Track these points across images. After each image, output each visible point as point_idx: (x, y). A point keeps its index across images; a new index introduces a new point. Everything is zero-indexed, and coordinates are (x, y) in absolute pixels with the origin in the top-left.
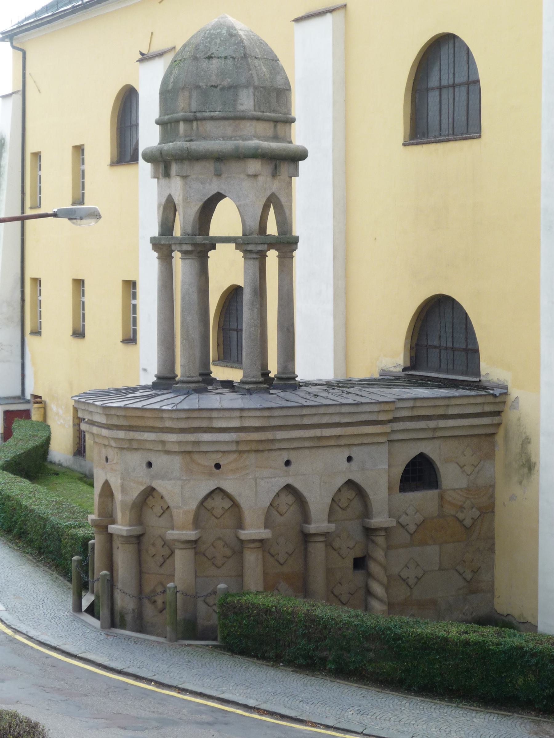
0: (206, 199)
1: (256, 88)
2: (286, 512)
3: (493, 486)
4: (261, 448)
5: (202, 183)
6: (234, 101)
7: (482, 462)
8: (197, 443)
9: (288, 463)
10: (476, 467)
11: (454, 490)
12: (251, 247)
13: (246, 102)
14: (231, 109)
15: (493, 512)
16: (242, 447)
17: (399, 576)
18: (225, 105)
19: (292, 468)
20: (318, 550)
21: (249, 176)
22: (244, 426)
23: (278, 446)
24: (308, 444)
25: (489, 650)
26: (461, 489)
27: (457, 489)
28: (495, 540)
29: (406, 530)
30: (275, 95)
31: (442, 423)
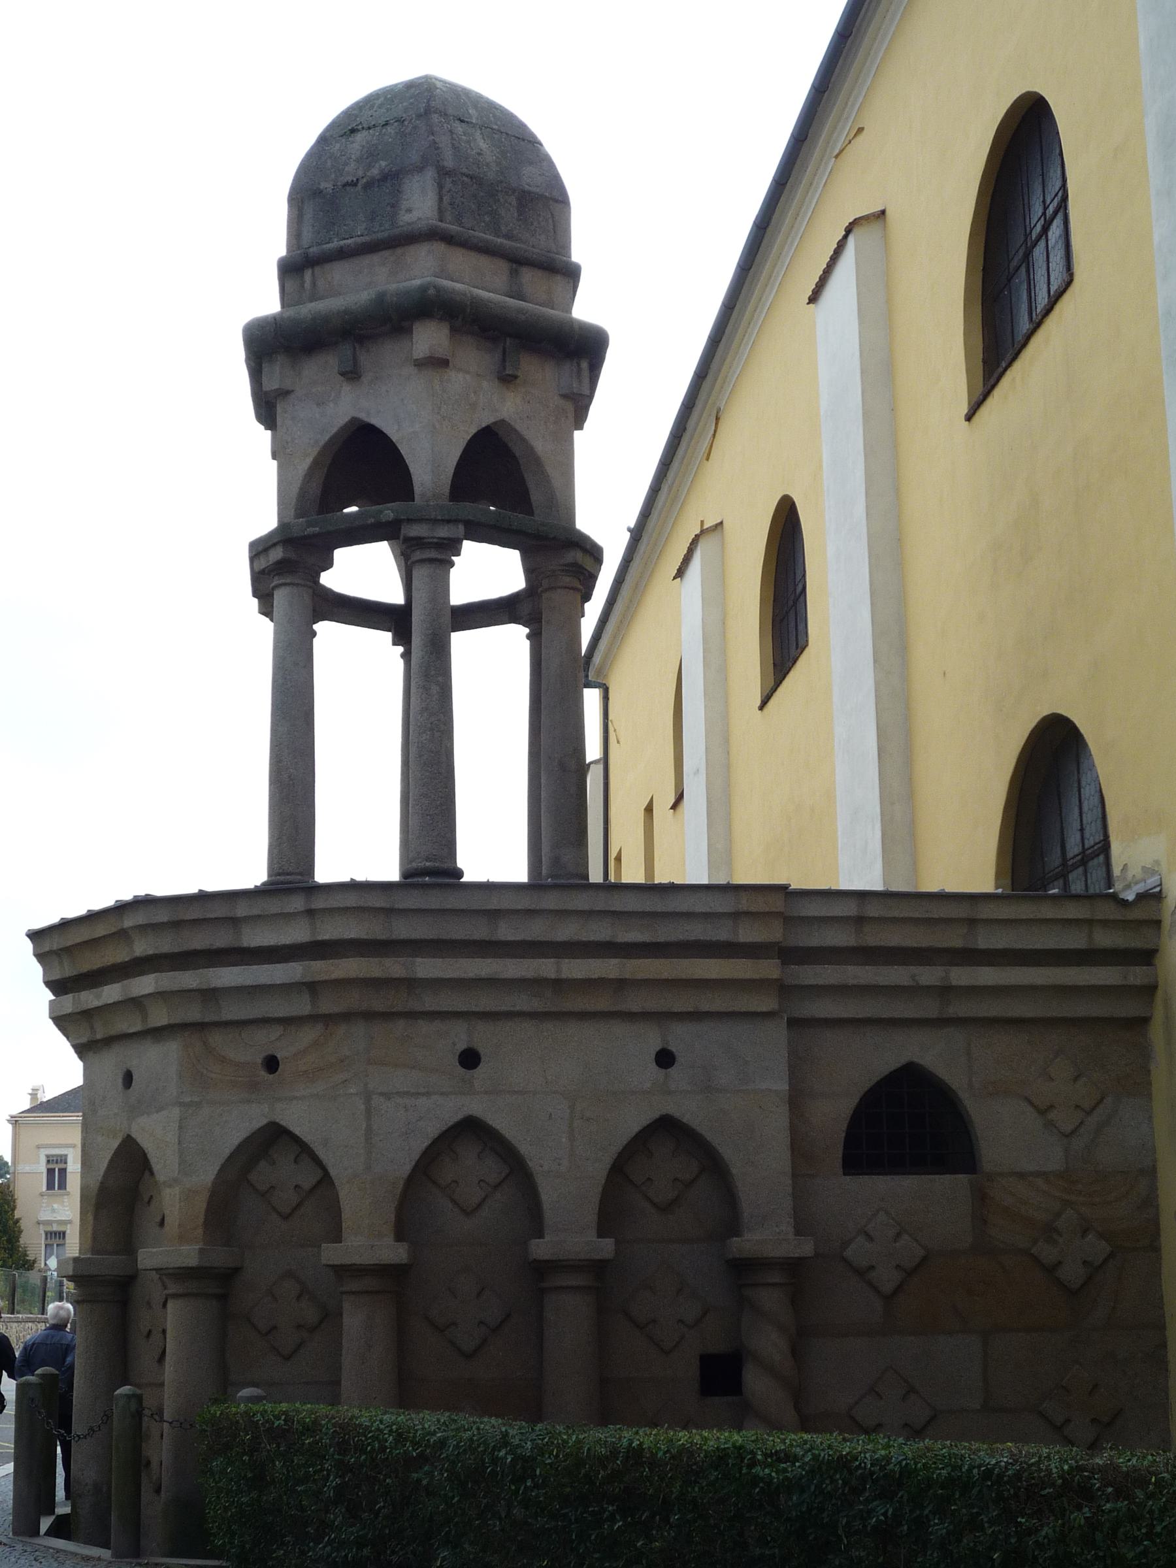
0: (327, 438)
1: (443, 173)
2: (479, 1206)
3: (1151, 1172)
4: (378, 1004)
5: (318, 405)
6: (393, 206)
7: (1109, 1100)
8: (210, 995)
9: (470, 1059)
10: (1089, 1113)
11: (1021, 1176)
12: (415, 531)
13: (420, 203)
14: (387, 226)
15: (1155, 1248)
16: (328, 1005)
17: (852, 1418)
18: (372, 220)
19: (481, 1071)
20: (569, 1318)
21: (421, 364)
22: (320, 938)
23: (430, 1002)
24: (522, 1002)
25: (756, 1480)
26: (1043, 1175)
27: (1038, 1174)
28: (1168, 1333)
29: (870, 1284)
30: (514, 203)
31: (961, 976)
